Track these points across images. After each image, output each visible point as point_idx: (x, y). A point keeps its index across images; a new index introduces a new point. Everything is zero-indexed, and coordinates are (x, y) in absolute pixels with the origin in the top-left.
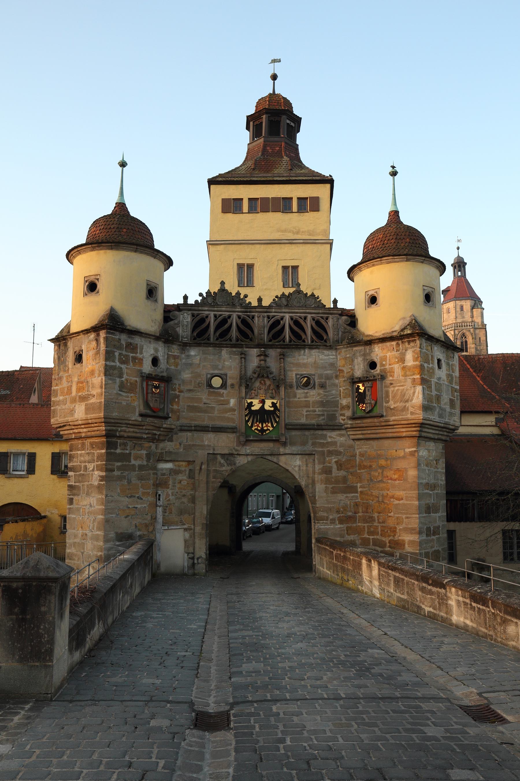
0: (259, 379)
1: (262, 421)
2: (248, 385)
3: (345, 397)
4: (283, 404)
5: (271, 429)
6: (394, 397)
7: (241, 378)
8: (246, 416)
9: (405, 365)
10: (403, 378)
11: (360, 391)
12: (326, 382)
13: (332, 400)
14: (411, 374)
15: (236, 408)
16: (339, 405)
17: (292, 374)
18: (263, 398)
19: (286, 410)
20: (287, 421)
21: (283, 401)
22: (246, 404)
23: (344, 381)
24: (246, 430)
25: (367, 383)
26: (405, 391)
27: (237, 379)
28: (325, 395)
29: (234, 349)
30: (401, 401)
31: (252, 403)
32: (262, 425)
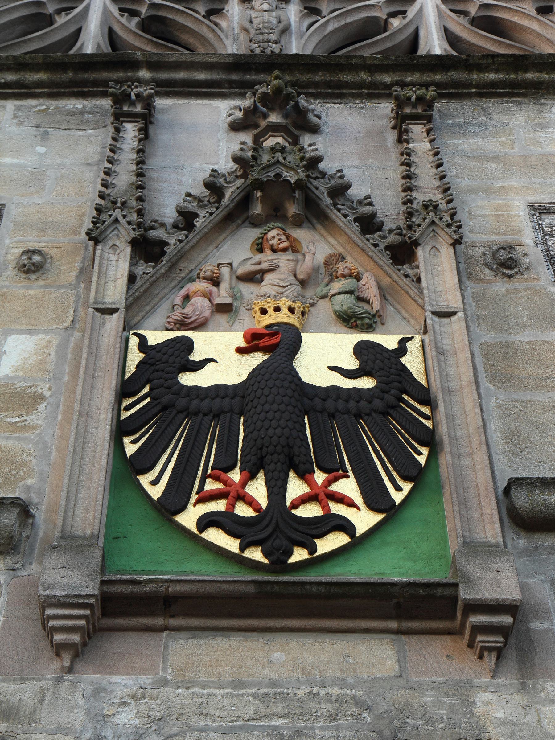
1: (277, 459)
5: (364, 520)
15: (44, 388)
19: (492, 403)
22: (135, 357)
27: (74, 232)
32: (277, 490)
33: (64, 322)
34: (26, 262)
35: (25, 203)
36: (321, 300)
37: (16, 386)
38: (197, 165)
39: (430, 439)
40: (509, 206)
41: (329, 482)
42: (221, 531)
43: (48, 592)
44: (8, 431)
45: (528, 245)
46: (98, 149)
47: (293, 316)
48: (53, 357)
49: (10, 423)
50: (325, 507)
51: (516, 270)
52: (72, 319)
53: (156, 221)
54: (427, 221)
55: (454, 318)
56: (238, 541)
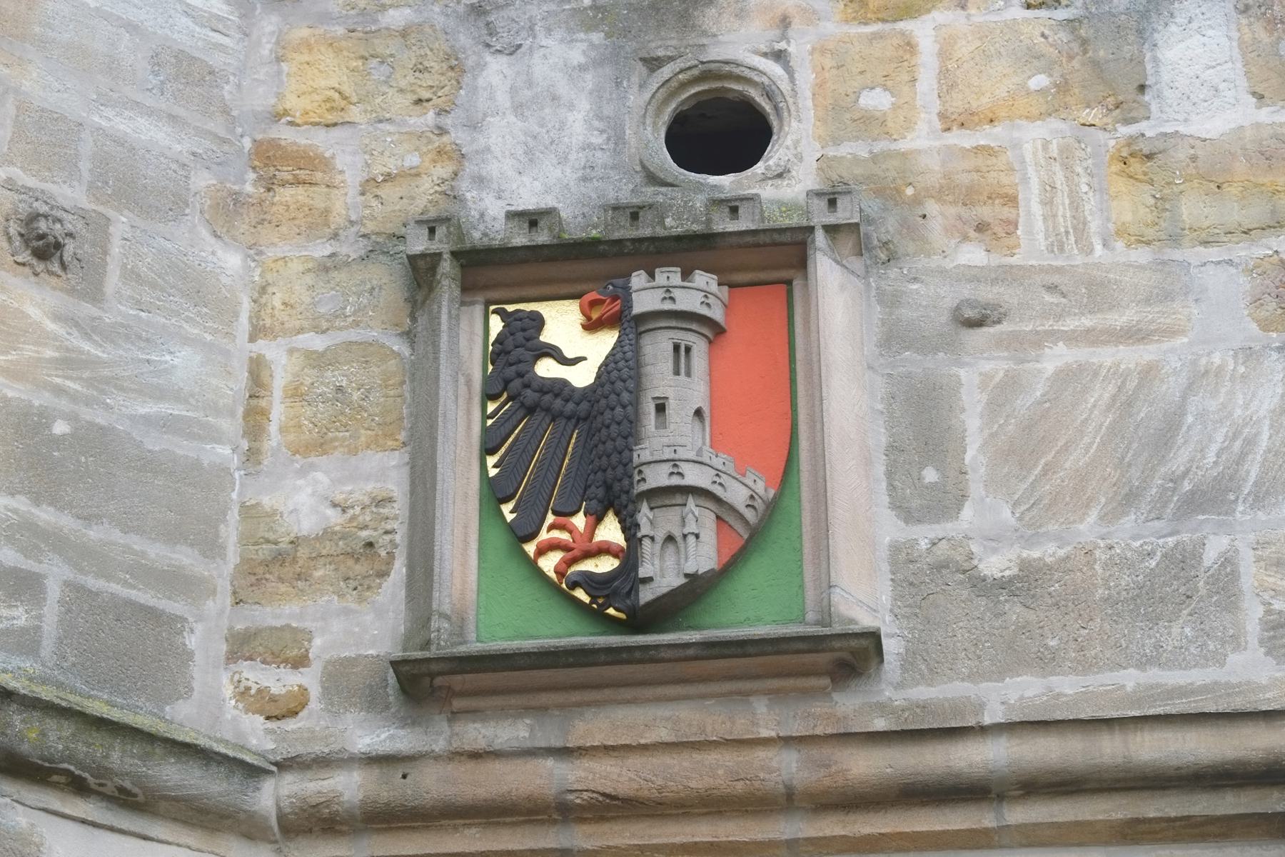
3: (321, 446)
6: (1021, 451)
9: (1148, 128)
10: (1142, 255)
11: (546, 369)
12: (100, 226)
13: (154, 443)
14: (1255, 213)
16: (230, 532)
23: (326, 267)
25: (669, 276)
26: (1170, 388)
28: (70, 362)
30: (1130, 499)
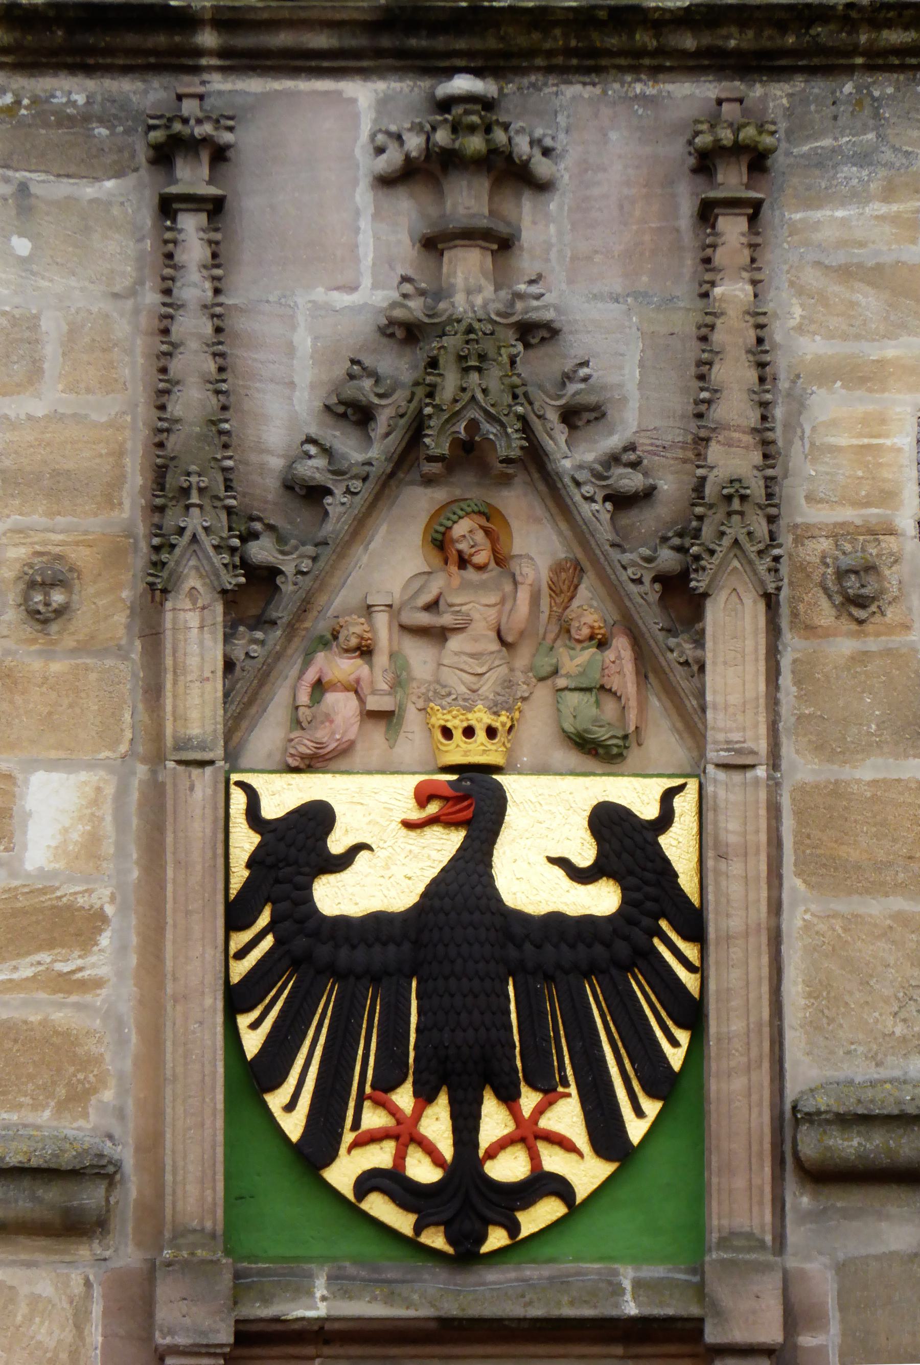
0: (419, 503)
1: (465, 1071)
2: (264, 579)
4: (740, 819)
5: (586, 1173)
7: (166, 486)
8: (238, 999)
15: (102, 897)
17: (877, 423)
18: (479, 751)
19: (794, 921)
20: (805, 1072)
21: (739, 800)
22: (245, 841)
24: (235, 1197)
29: (72, 91)
31: (317, 818)
32: (465, 1125)
33: (118, 742)
34: (41, 608)
35: (12, 415)
36: (540, 684)
37: (59, 894)
38: (319, 294)
39: (690, 1013)
40: (883, 421)
41: (540, 1111)
42: (386, 1198)
43: (168, 1340)
44: (60, 991)
45: (903, 535)
46: (131, 248)
47: (494, 748)
48: (108, 826)
49: (61, 975)
50: (535, 1158)
51: (873, 608)
52: (130, 736)
53: (259, 519)
54: (726, 542)
55: (750, 774)
56: (412, 1218)
